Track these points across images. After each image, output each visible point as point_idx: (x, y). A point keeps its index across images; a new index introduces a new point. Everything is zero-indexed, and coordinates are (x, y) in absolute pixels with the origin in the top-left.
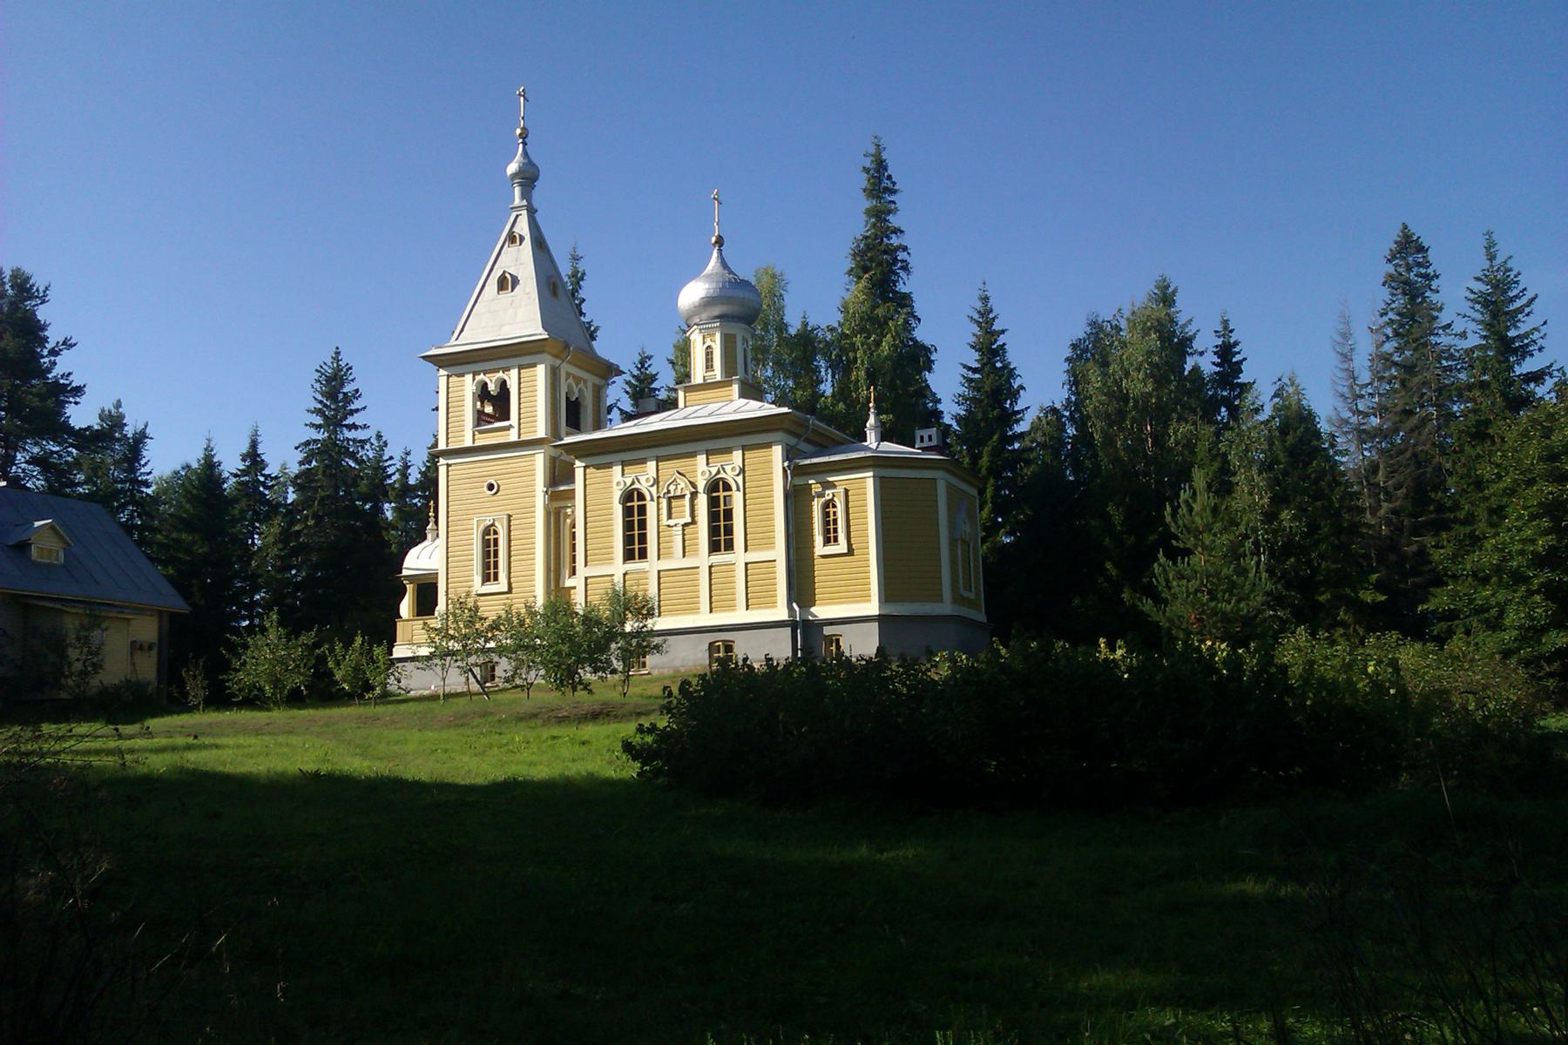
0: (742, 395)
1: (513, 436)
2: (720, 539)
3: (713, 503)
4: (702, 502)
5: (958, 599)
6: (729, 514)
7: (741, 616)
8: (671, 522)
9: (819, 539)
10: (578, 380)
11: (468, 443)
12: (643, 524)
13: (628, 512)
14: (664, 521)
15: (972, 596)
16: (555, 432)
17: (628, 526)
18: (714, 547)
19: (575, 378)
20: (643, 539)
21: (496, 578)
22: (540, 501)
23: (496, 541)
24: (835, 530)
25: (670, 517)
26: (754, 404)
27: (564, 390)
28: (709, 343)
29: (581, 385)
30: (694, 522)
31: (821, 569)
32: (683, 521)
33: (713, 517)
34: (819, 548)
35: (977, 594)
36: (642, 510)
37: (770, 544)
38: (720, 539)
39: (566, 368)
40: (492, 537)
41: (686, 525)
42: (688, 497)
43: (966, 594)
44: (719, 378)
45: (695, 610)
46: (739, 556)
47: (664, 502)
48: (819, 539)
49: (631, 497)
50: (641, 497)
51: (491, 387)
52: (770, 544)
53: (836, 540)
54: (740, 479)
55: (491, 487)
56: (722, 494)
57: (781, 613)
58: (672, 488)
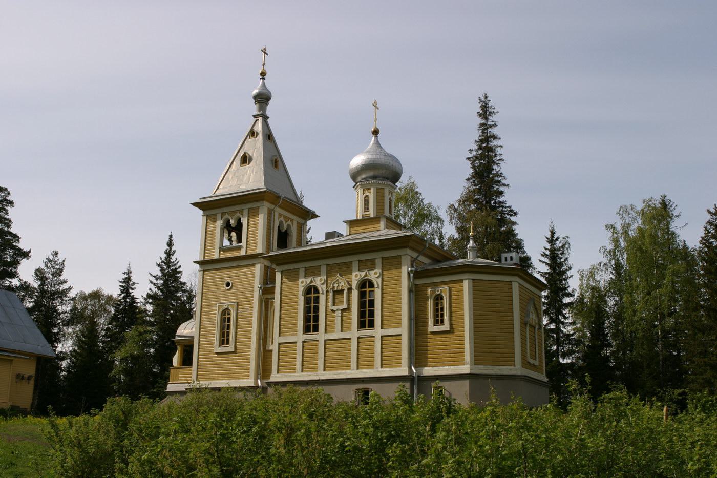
0: (387, 227)
1: (243, 252)
2: (366, 320)
3: (362, 295)
4: (355, 294)
5: (526, 364)
6: (372, 303)
7: (377, 372)
8: (335, 308)
9: (431, 321)
10: (287, 219)
11: (216, 256)
12: (317, 309)
13: (307, 301)
14: (331, 307)
15: (537, 363)
16: (269, 248)
17: (307, 310)
18: (362, 325)
19: (285, 217)
20: (316, 318)
21: (228, 343)
22: (256, 294)
23: (229, 319)
24: (442, 315)
25: (334, 304)
26: (392, 231)
27: (277, 224)
28: (366, 193)
29: (289, 222)
30: (348, 309)
31: (432, 341)
32: (341, 307)
33: (362, 305)
34: (432, 328)
35: (541, 362)
36: (317, 300)
37: (398, 324)
38: (366, 320)
39: (278, 210)
40: (227, 316)
41: (343, 310)
42: (345, 292)
43: (532, 361)
44: (372, 216)
45: (348, 367)
46: (377, 332)
47: (331, 295)
48: (431, 321)
49: (311, 290)
50: (316, 291)
51: (232, 222)
52: (398, 324)
53: (442, 321)
54: (380, 280)
55: (228, 285)
56: (368, 290)
57: (403, 371)
58: (336, 285)
